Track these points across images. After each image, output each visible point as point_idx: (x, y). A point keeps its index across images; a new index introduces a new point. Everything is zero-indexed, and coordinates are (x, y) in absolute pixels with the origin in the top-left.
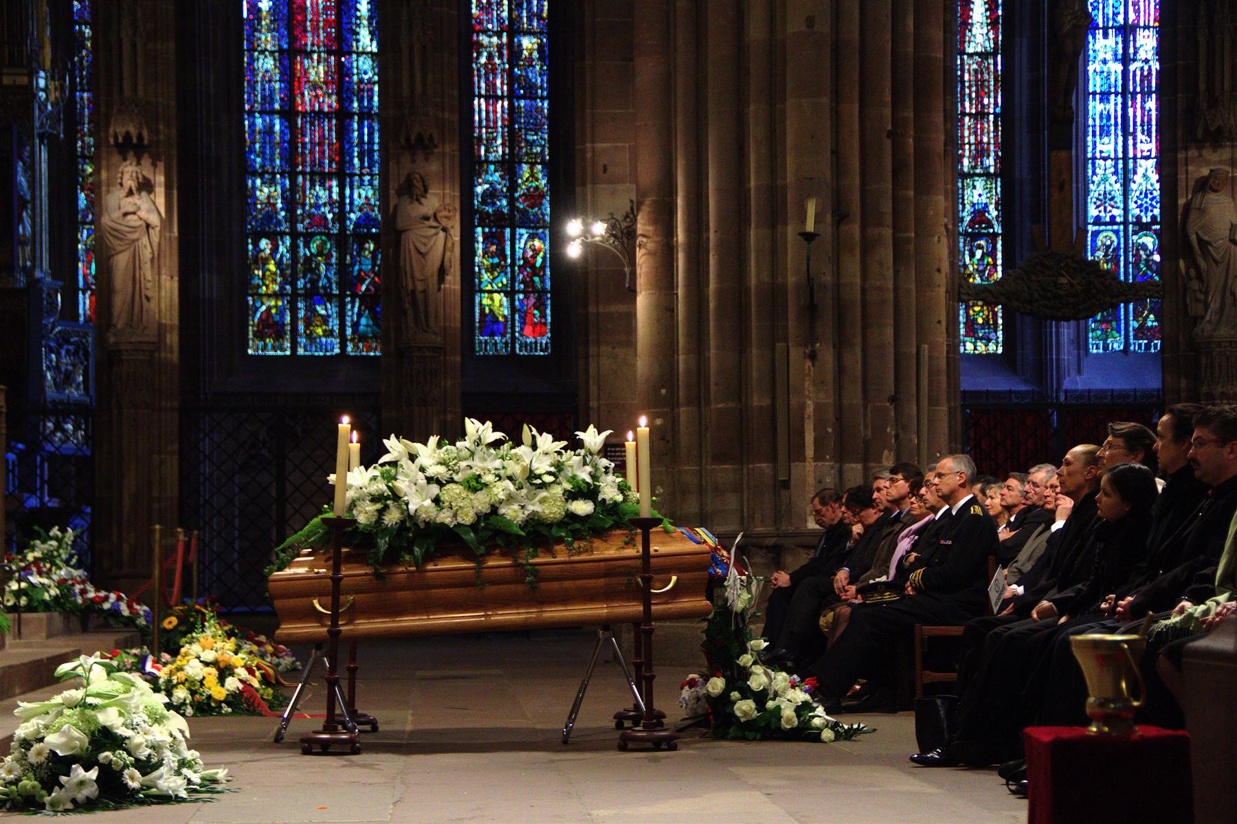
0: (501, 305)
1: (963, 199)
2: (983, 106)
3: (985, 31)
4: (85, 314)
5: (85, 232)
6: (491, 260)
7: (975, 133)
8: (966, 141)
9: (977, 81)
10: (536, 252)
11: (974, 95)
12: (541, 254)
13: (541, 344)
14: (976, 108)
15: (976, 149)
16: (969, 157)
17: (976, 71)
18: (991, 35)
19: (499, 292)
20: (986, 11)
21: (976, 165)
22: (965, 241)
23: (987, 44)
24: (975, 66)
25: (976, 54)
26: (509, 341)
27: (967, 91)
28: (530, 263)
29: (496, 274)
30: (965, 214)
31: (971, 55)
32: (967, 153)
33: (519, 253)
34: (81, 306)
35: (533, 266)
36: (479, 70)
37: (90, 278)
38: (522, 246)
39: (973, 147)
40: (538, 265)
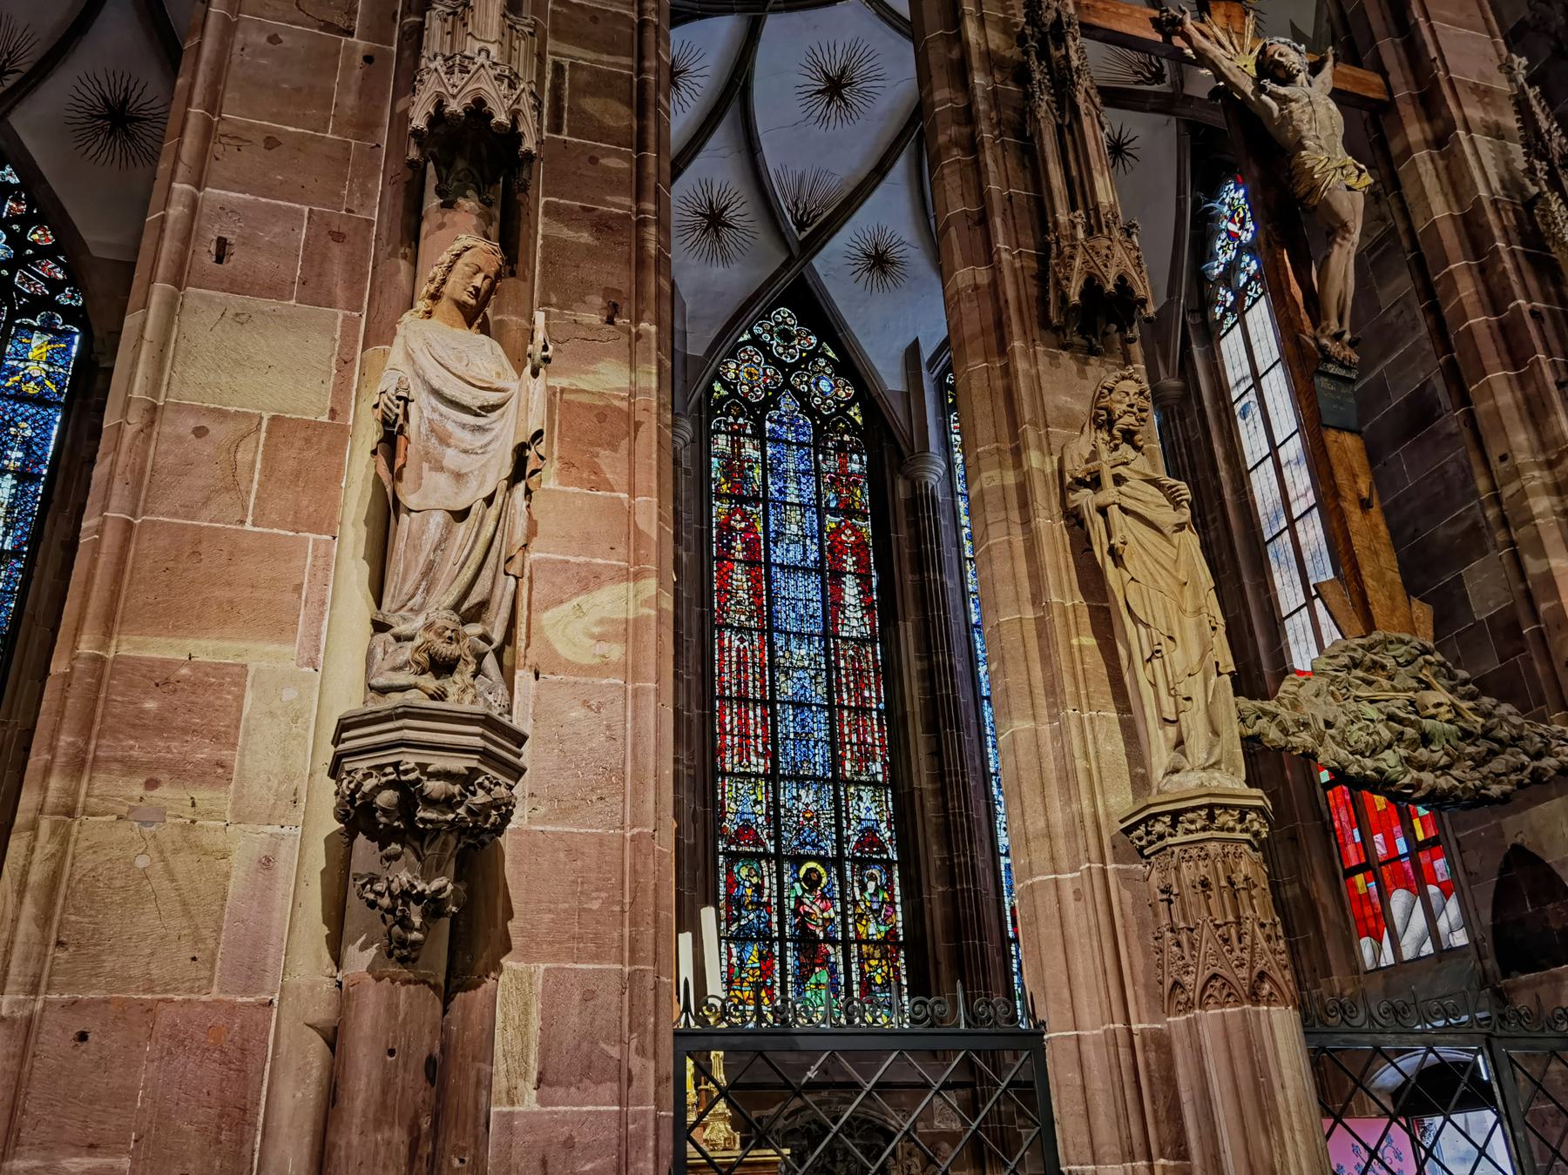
1: (847, 812)
2: (864, 699)
3: (859, 615)
7: (857, 731)
9: (854, 669)
14: (856, 701)
15: (859, 751)
16: (851, 760)
17: (852, 658)
20: (860, 593)
21: (860, 770)
22: (853, 868)
23: (863, 629)
25: (851, 638)
30: (850, 832)
31: (845, 640)
32: (849, 755)
39: (856, 748)
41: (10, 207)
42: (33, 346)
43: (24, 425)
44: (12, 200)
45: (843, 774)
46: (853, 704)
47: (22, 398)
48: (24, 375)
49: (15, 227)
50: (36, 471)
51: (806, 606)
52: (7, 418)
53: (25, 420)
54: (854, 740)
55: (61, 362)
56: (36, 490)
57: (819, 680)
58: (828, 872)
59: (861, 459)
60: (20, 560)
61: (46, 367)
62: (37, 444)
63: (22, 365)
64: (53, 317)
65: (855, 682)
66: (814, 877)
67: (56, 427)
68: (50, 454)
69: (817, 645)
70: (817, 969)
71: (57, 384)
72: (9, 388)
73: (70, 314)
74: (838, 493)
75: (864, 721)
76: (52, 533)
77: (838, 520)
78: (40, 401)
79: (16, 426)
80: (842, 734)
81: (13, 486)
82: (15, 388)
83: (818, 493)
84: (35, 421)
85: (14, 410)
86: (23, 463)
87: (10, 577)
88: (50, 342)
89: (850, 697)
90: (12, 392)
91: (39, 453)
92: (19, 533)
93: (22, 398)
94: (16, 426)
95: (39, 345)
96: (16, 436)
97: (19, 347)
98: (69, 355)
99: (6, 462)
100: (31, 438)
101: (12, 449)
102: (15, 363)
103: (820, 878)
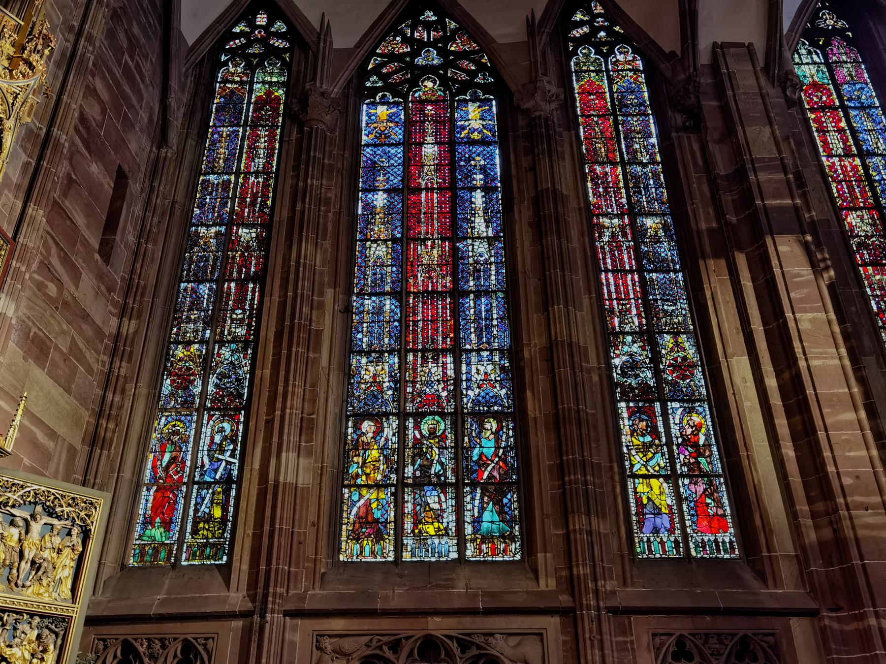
4: (145, 514)
5: (164, 419)
6: (641, 439)
10: (698, 428)
12: (703, 430)
13: (724, 542)
19: (657, 477)
26: (680, 539)
28: (689, 442)
29: (650, 455)
33: (675, 430)
34: (142, 506)
35: (696, 445)
36: (602, 247)
37: (160, 471)
38: (677, 421)
40: (701, 442)
41: (434, 35)
42: (470, 111)
43: (478, 158)
44: (434, 31)
47: (473, 143)
48: (470, 129)
49: (440, 45)
50: (494, 185)
52: (467, 156)
53: (478, 155)
55: (489, 118)
56: (497, 197)
60: (500, 242)
61: (481, 122)
62: (490, 169)
63: (467, 123)
64: (476, 92)
67: (497, 157)
68: (499, 174)
71: (490, 131)
72: (463, 138)
73: (486, 88)
76: (521, 219)
78: (483, 142)
79: (474, 159)
81: (483, 197)
82: (466, 137)
84: (484, 155)
85: (470, 151)
86: (485, 181)
87: (497, 253)
88: (479, 107)
90: (466, 140)
91: (492, 174)
92: (495, 225)
93: (473, 143)
94: (474, 159)
95: (473, 110)
96: (476, 166)
97: (462, 113)
98: (492, 112)
99: (475, 182)
100: (485, 165)
101: (476, 174)
102: (462, 123)
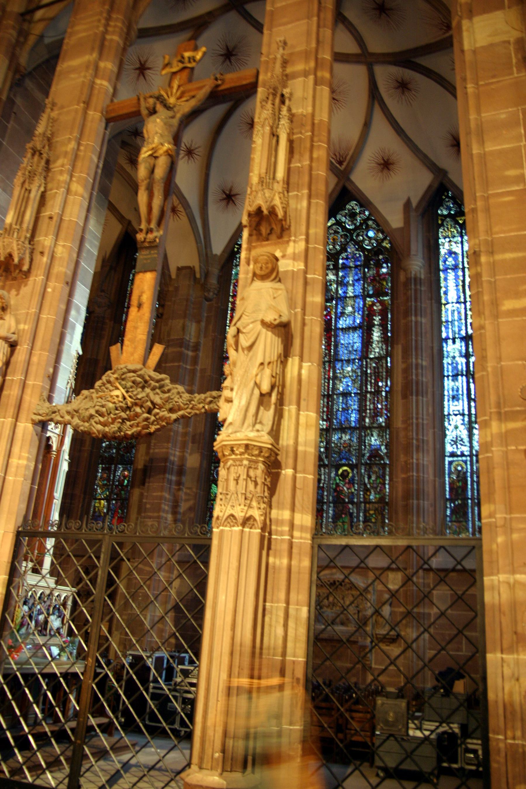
0: (104, 507)
1: (365, 442)
8: (368, 407)
9: (375, 372)
10: (125, 477)
11: (373, 381)
15: (374, 413)
17: (374, 367)
18: (384, 347)
19: (103, 499)
21: (374, 421)
24: (374, 365)
25: (375, 358)
27: (369, 379)
30: (366, 452)
31: (371, 359)
32: (368, 415)
39: (372, 411)
45: (365, 425)
46: (373, 390)
51: (353, 347)
54: (372, 406)
57: (357, 380)
58: (352, 470)
59: (388, 266)
65: (375, 380)
66: (345, 473)
69: (357, 364)
70: (343, 516)
74: (374, 287)
75: (378, 398)
77: (372, 299)
80: (366, 405)
83: (364, 289)
89: (371, 386)
103: (348, 473)
